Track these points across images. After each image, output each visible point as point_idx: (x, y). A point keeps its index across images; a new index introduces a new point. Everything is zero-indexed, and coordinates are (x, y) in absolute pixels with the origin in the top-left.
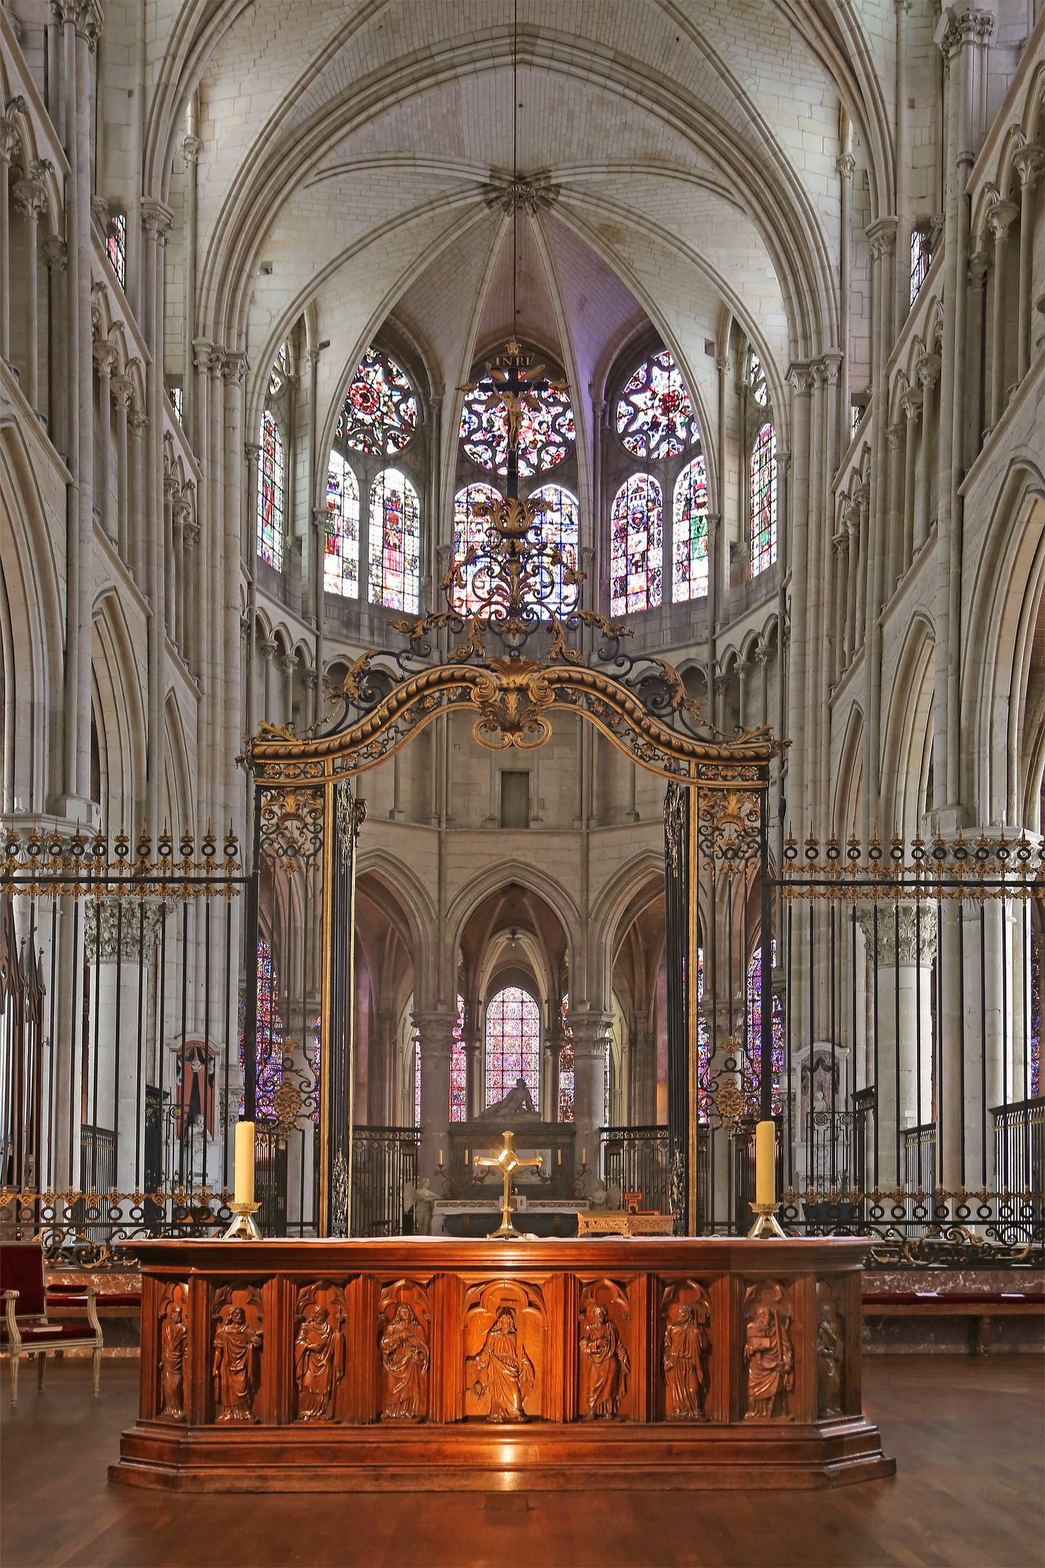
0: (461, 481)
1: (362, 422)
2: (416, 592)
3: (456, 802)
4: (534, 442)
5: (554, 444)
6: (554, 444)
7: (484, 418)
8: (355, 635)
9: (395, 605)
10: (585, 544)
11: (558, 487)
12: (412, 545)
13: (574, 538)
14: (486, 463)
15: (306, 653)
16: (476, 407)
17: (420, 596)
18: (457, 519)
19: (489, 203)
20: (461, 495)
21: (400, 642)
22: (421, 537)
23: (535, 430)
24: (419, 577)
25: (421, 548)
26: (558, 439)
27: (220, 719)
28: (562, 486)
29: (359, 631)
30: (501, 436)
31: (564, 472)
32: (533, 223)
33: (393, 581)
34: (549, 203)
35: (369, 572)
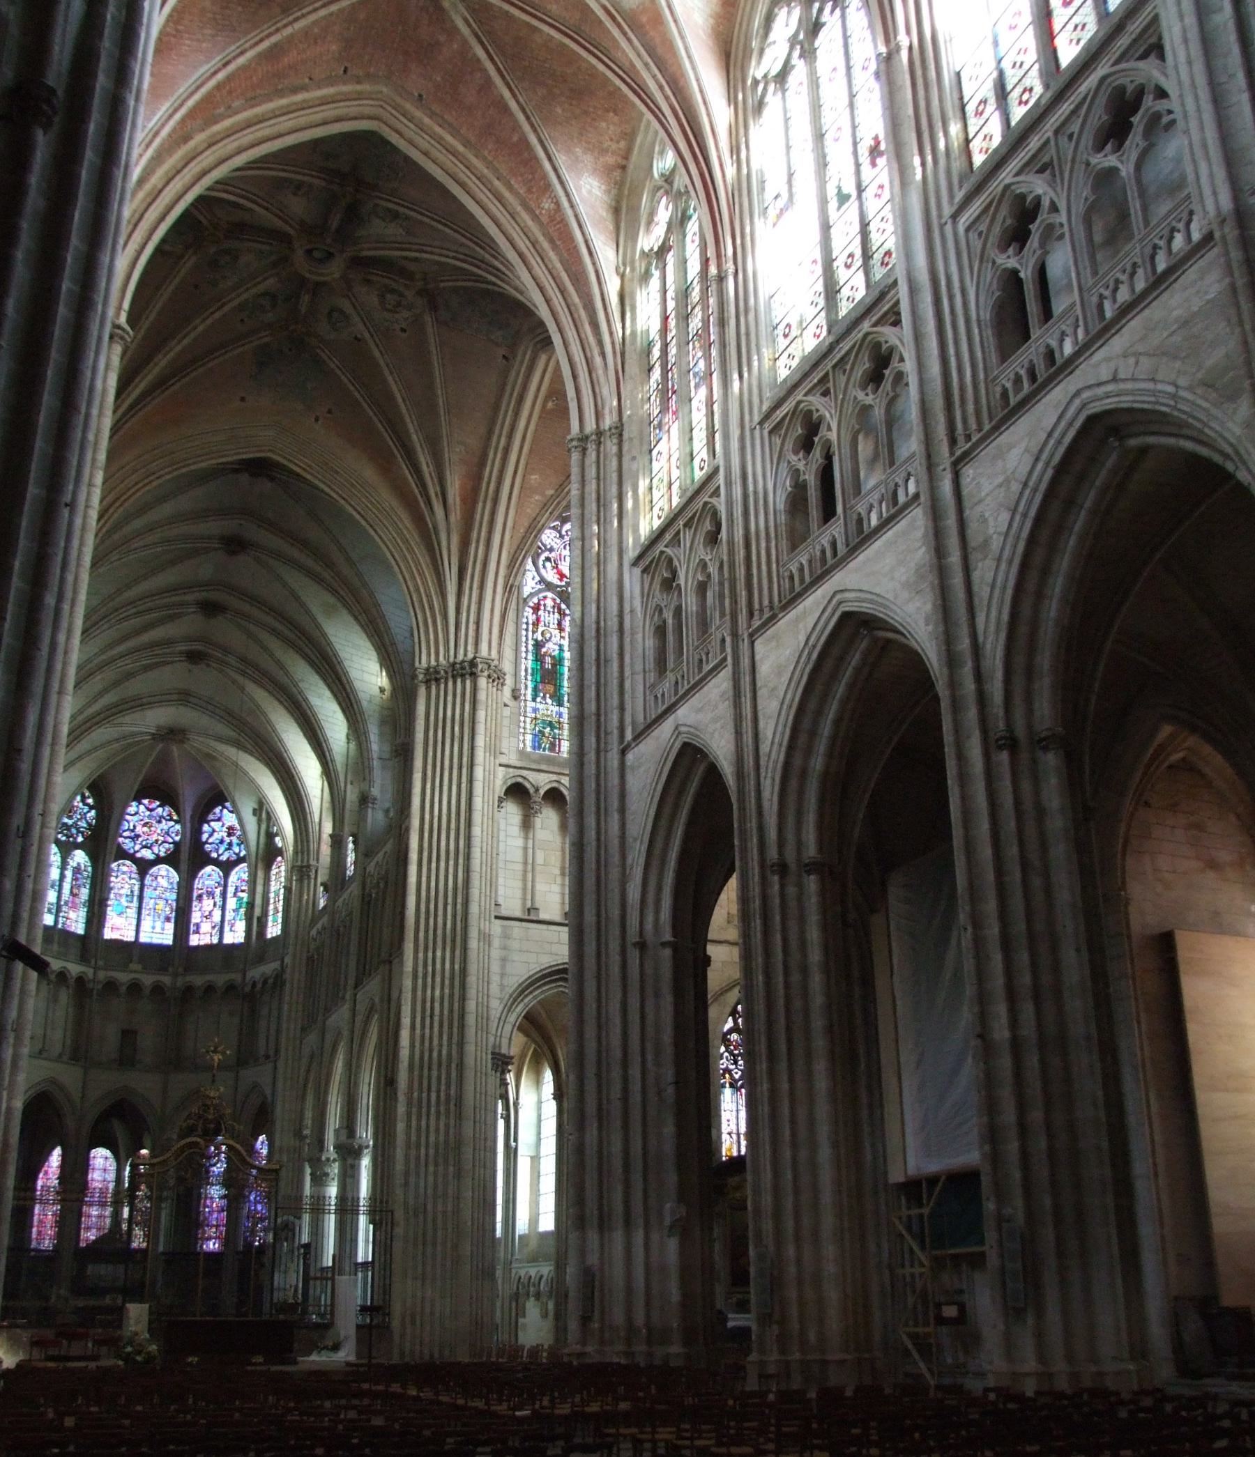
4: (157, 841)
13: (174, 896)
20: (114, 865)
30: (138, 836)
31: (171, 859)
32: (175, 749)
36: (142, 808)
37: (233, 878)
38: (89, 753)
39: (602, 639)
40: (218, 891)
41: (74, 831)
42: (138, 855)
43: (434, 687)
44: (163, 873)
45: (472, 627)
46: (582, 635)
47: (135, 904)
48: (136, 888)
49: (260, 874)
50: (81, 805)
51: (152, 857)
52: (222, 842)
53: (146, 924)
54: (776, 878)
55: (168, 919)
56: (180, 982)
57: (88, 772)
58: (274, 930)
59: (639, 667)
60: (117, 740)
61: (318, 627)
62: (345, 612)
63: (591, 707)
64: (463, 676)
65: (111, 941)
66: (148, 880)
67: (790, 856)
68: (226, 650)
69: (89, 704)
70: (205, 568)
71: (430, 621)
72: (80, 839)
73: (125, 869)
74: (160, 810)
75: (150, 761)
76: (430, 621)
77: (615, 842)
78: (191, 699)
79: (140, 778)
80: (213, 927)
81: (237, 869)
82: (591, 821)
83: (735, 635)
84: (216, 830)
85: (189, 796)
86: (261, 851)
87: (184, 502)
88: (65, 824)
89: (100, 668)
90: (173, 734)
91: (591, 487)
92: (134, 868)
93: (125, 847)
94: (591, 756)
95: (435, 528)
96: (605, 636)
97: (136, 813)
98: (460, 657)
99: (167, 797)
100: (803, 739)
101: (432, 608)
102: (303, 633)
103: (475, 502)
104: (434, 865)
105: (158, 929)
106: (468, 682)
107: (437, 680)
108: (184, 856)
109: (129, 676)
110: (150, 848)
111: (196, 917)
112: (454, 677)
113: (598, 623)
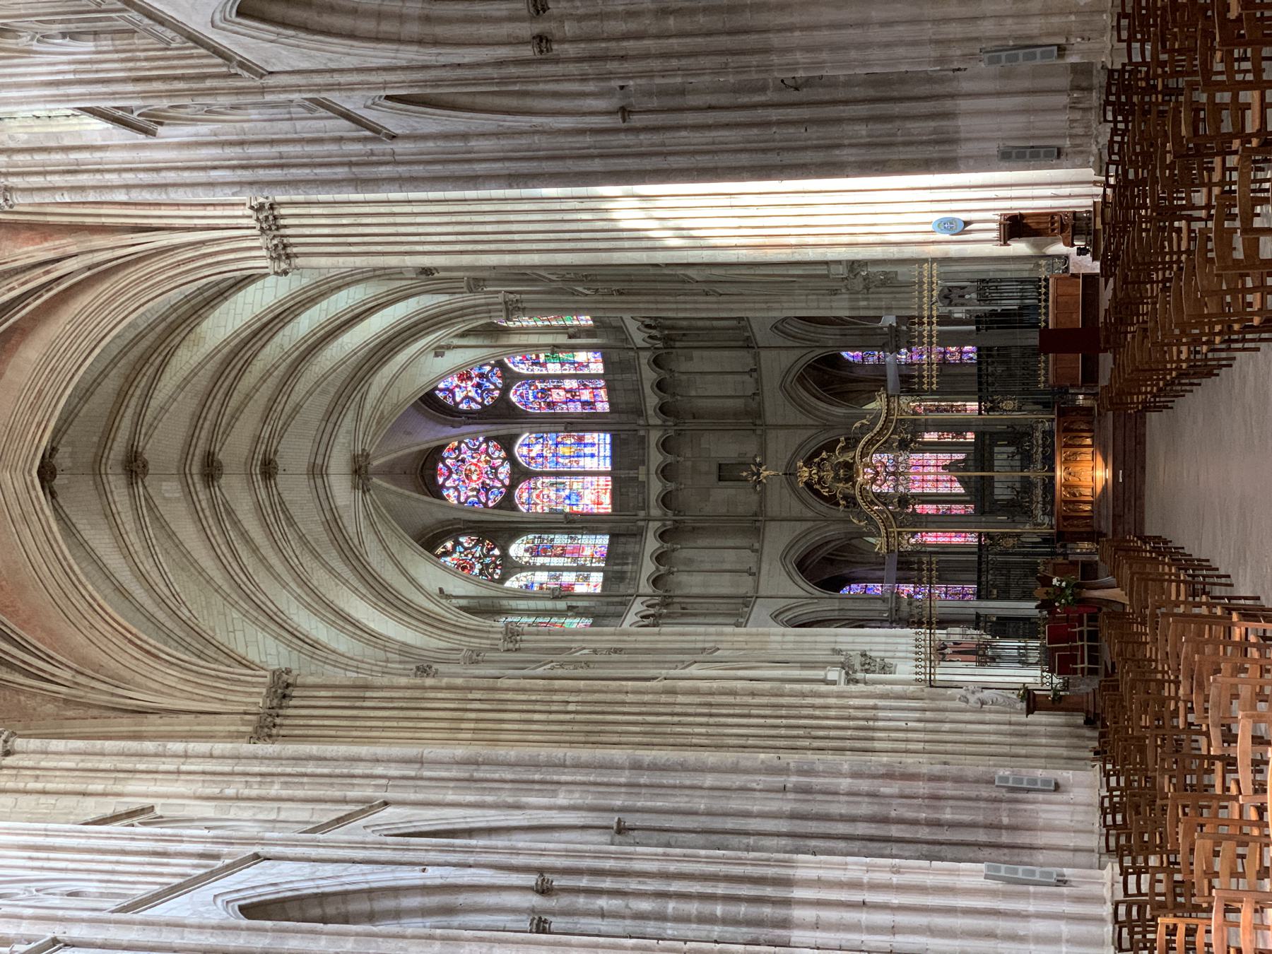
0: (514, 508)
1: (481, 570)
2: (594, 537)
3: (741, 510)
4: (487, 462)
5: (487, 449)
6: (487, 449)
7: (470, 494)
8: (629, 575)
9: (604, 550)
10: (563, 428)
11: (517, 446)
12: (560, 540)
13: (554, 435)
14: (501, 493)
15: (649, 603)
16: (462, 499)
17: (596, 534)
18: (540, 511)
19: (369, 490)
20: (523, 509)
21: (632, 547)
22: (554, 533)
23: (478, 461)
24: (582, 534)
25: (562, 533)
26: (484, 446)
27: (729, 638)
28: (515, 442)
29: (625, 572)
30: (483, 483)
31: (507, 443)
33: (588, 552)
34: (368, 455)
35: (583, 565)
36: (448, 483)
37: (523, 369)
38: (397, 564)
39: (253, 162)
40: (540, 385)
41: (488, 560)
42: (507, 482)
43: (295, 250)
44: (525, 450)
45: (210, 211)
46: (251, 184)
47: (566, 480)
48: (547, 480)
49: (515, 340)
50: (455, 556)
51: (507, 466)
52: (479, 386)
53: (589, 464)
54: (555, 47)
55: (580, 442)
56: (655, 421)
57: (417, 557)
58: (586, 321)
59: (286, 126)
60: (377, 533)
61: (217, 350)
62: (198, 330)
63: (341, 172)
64: (275, 218)
65: (613, 503)
66: (533, 467)
67: (526, 29)
68: (257, 439)
69: (346, 582)
70: (167, 491)
71: (210, 260)
72: (497, 552)
73: (525, 495)
74: (448, 462)
75: (394, 488)
76: (210, 260)
77: (505, 143)
78: (319, 461)
79: (416, 495)
80: (586, 387)
81: (511, 365)
82: (480, 168)
83: (263, 90)
84: (464, 394)
85: (428, 434)
86: (487, 342)
87: (101, 542)
88: (481, 573)
89: (304, 583)
90: (360, 471)
91: (57, 180)
92: (523, 485)
93: (499, 498)
94: (402, 170)
95: (89, 268)
96: (250, 158)
97: (456, 488)
98: (252, 222)
99: (433, 456)
100: (387, 27)
101: (192, 260)
102: (227, 362)
103: (47, 225)
104: (516, 237)
105: (594, 450)
106: (283, 211)
107: (285, 246)
108: (503, 430)
109: (302, 537)
110: (496, 469)
111: (575, 408)
112: (278, 228)
113: (233, 168)
